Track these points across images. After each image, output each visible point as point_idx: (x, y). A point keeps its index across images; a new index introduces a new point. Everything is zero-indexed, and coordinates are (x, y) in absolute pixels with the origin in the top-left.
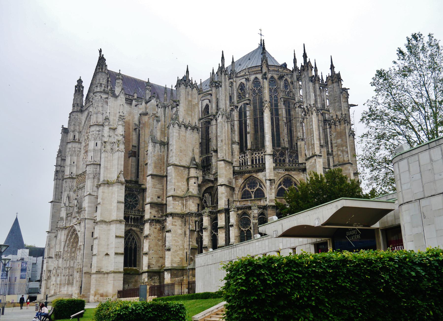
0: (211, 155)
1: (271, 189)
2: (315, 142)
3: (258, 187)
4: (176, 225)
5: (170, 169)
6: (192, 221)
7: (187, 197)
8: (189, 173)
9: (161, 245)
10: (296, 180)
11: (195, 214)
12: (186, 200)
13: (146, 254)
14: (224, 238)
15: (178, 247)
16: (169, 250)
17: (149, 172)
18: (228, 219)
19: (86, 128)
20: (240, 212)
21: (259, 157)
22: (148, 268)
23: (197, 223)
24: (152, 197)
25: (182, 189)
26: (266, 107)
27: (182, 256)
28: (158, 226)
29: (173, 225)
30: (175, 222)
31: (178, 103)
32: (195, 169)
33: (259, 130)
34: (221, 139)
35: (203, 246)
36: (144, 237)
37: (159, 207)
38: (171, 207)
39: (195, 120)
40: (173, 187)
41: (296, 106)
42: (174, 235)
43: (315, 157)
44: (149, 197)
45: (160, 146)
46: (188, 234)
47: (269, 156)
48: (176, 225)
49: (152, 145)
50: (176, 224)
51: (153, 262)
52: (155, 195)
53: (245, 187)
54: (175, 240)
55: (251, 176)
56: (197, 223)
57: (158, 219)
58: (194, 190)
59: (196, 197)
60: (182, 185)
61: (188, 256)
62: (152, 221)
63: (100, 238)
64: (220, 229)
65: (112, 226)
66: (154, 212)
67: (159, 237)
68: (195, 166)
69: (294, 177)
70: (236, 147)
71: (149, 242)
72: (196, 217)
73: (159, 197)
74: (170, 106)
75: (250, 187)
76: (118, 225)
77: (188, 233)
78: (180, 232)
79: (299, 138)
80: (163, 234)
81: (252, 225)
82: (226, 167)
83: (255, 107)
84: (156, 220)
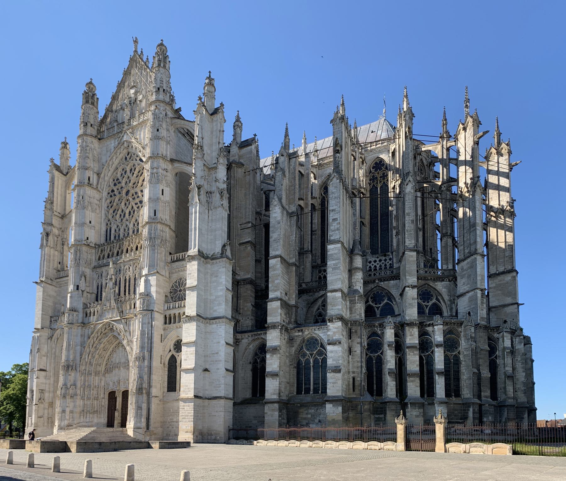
12: (351, 301)
14: (418, 363)
16: (337, 370)
19: (112, 170)
44: (276, 291)
46: (359, 352)
50: (344, 334)
51: (283, 389)
57: (286, 325)
61: (357, 383)
62: (285, 329)
63: (197, 343)
65: (214, 326)
73: (286, 294)
76: (228, 326)
77: (357, 349)
78: (346, 346)
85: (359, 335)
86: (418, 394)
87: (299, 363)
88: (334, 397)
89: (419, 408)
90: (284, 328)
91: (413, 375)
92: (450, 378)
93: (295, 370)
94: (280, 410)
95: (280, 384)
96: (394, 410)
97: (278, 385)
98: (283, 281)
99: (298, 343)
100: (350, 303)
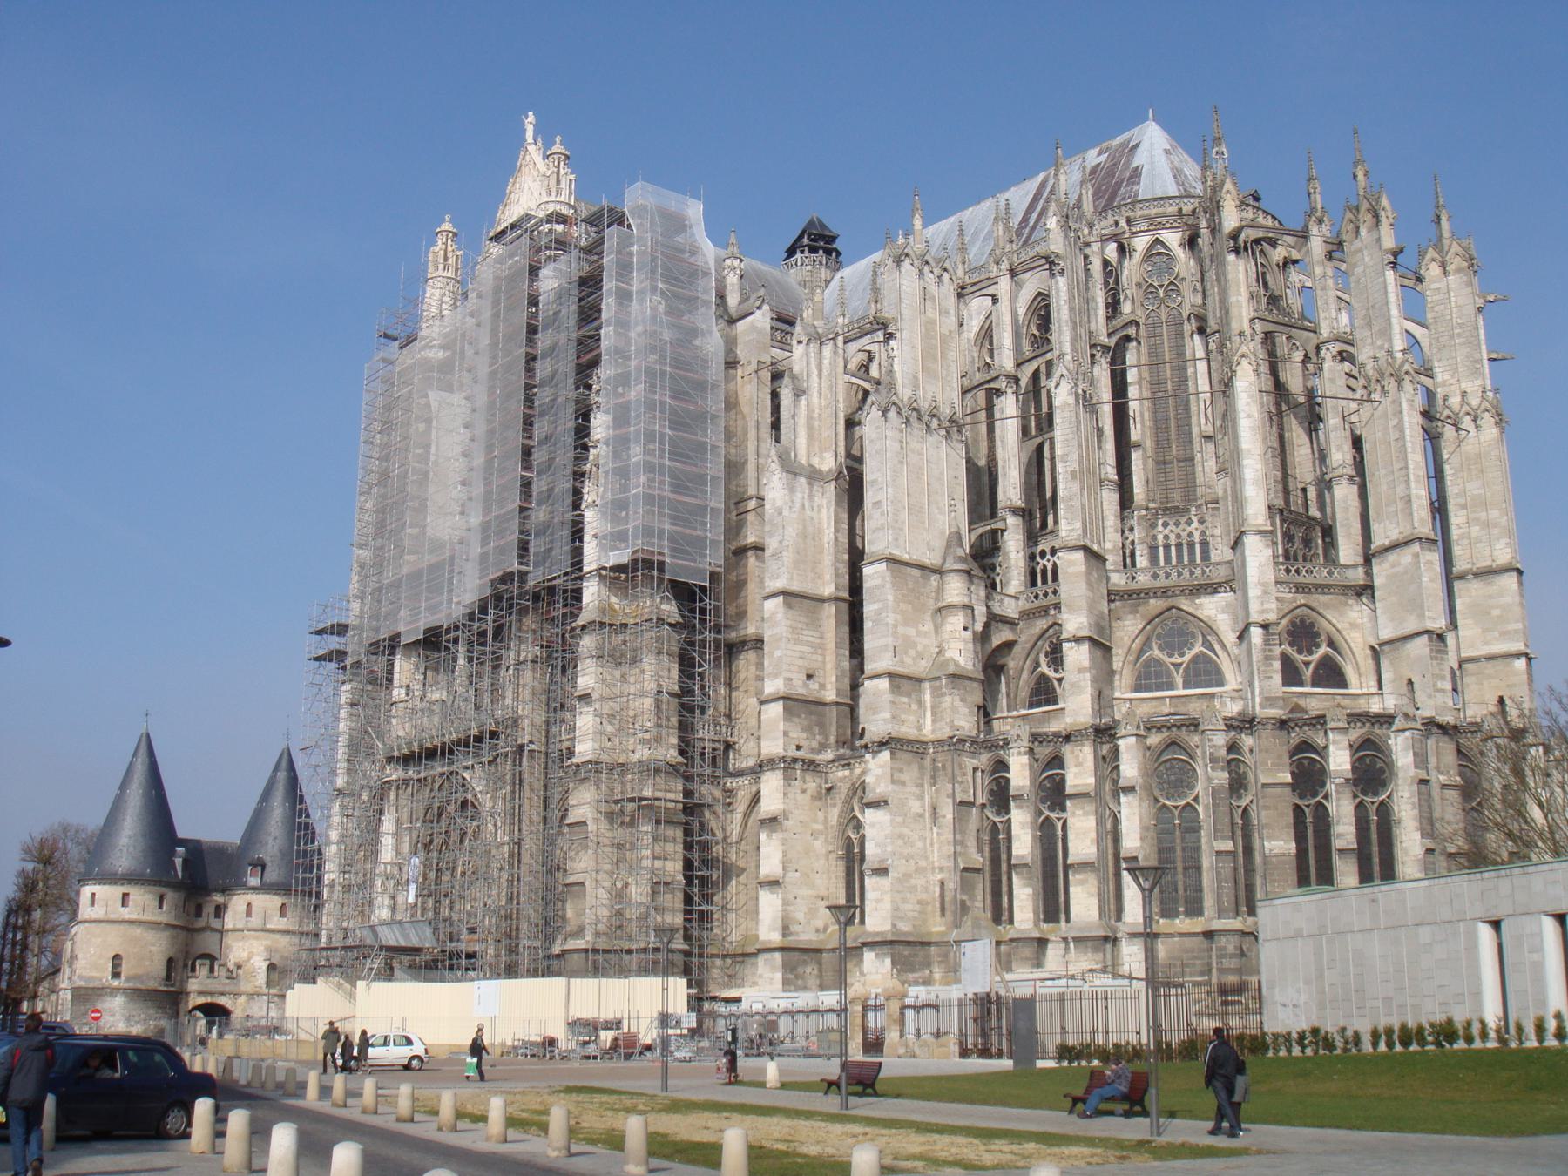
0: (999, 525)
1: (1268, 659)
2: (1414, 491)
3: (1198, 648)
4: (903, 783)
5: (872, 573)
6: (961, 768)
7: (939, 678)
8: (940, 590)
9: (824, 851)
10: (1334, 626)
11: (973, 743)
13: (774, 883)
14: (1093, 835)
15: (912, 862)
16: (882, 871)
17: (779, 584)
18: (1108, 762)
20: (1154, 739)
21: (1179, 536)
22: (784, 935)
23: (979, 774)
24: (788, 675)
25: (920, 648)
26: (1243, 356)
27: (924, 896)
28: (812, 784)
29: (893, 782)
30: (901, 770)
31: (890, 329)
32: (965, 576)
33: (1173, 436)
34: (1070, 469)
35: (1013, 862)
36: (762, 821)
37: (811, 713)
38: (887, 715)
39: (946, 395)
40: (890, 641)
41: (1323, 352)
42: (899, 819)
43: (1416, 547)
44: (776, 676)
45: (809, 484)
46: (950, 817)
47: (1257, 537)
48: (903, 783)
49: (784, 481)
50: (903, 777)
51: (800, 916)
52: (796, 668)
53: (1146, 644)
54: (900, 836)
55: (1169, 609)
56: (979, 774)
58: (961, 653)
59: (971, 679)
60: (918, 633)
64: (1075, 801)
66: (797, 735)
67: (816, 821)
68: (964, 567)
69: (1328, 616)
70: (1110, 499)
71: (784, 842)
72: (973, 754)
73: (809, 677)
74: (840, 339)
75: (1169, 648)
77: (947, 812)
79: (1340, 471)
80: (827, 812)
81: (1200, 788)
82: (1088, 573)
83: (1155, 351)
84: (803, 760)
85: (950, 775)
86: (1094, 913)
87: (849, 845)
88: (877, 934)
89: (1096, 950)
90: (798, 766)
91: (1084, 866)
92: (1175, 868)
93: (842, 863)
94: (788, 967)
95: (786, 903)
96: (1027, 959)
97: (780, 908)
98: (799, 648)
99: (843, 796)
100: (932, 693)
